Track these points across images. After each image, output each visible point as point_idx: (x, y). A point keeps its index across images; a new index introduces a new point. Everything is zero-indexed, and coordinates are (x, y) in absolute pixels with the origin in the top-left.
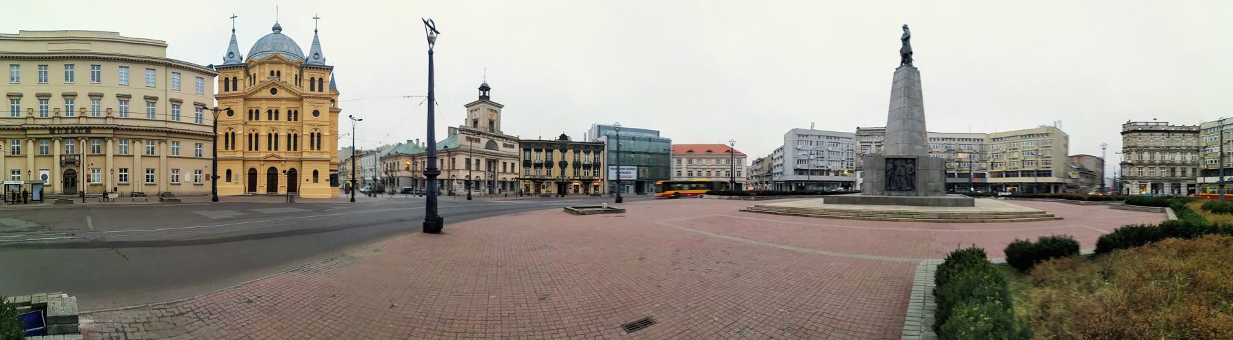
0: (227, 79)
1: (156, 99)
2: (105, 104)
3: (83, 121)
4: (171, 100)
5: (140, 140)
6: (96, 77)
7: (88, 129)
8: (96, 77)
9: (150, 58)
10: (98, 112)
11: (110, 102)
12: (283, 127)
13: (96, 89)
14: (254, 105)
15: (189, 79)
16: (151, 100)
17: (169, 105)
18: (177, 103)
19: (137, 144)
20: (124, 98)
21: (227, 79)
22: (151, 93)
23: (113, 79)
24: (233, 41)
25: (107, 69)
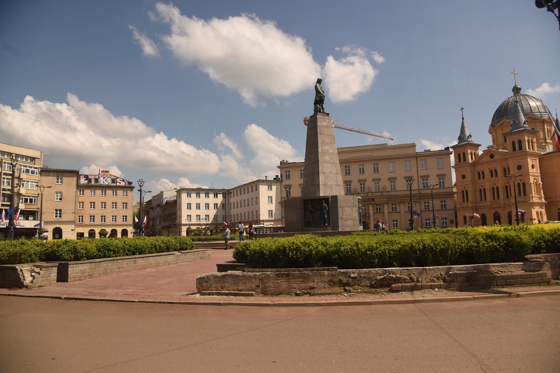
0: (459, 154)
1: (411, 177)
2: (382, 184)
3: (370, 195)
4: (421, 177)
5: (404, 203)
6: (376, 170)
7: (373, 200)
8: (376, 170)
9: (407, 154)
10: (379, 190)
11: (385, 184)
12: (500, 182)
13: (376, 176)
14: (480, 168)
15: (432, 162)
16: (409, 179)
17: (421, 180)
18: (425, 178)
19: (402, 205)
20: (392, 180)
21: (459, 154)
22: (408, 174)
23: (386, 170)
25: (382, 166)
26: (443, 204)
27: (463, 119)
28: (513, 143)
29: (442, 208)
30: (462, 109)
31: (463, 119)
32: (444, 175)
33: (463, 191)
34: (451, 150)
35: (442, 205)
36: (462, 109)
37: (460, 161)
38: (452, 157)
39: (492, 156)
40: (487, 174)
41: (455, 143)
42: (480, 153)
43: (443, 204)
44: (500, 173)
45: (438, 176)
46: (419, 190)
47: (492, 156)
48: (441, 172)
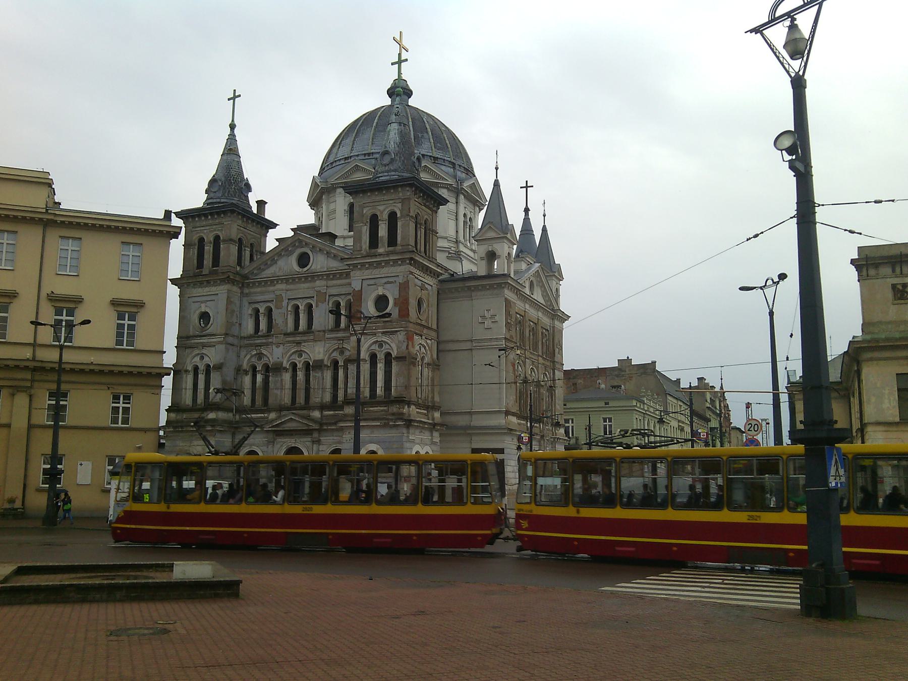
0: (201, 241)
4: (53, 298)
15: (102, 253)
18: (67, 304)
21: (201, 241)
24: (231, 150)
26: (121, 405)
27: (232, 127)
28: (374, 221)
29: (115, 420)
30: (235, 97)
31: (232, 127)
32: (140, 305)
33: (196, 369)
34: (176, 222)
35: (115, 410)
36: (235, 97)
37: (200, 264)
38: (177, 247)
39: (303, 260)
40: (284, 320)
41: (198, 200)
42: (271, 244)
43: (121, 405)
44: (322, 318)
45: (115, 303)
46: (34, 345)
47: (303, 260)
48: (128, 292)
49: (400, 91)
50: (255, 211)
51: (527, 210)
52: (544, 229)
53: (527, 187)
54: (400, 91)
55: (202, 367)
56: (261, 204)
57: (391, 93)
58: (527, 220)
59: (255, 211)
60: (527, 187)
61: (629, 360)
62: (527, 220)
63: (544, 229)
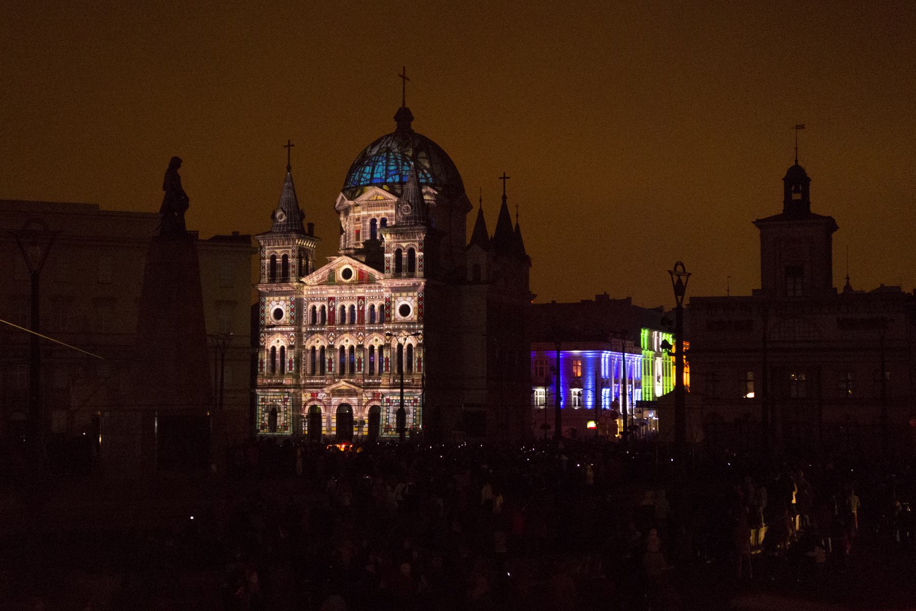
30: (289, 146)
31: (289, 168)
36: (289, 146)
49: (404, 116)
50: (307, 231)
51: (504, 198)
52: (517, 226)
53: (504, 178)
54: (404, 116)
55: (278, 349)
56: (311, 226)
57: (396, 118)
58: (504, 208)
59: (307, 231)
60: (504, 178)
61: (606, 296)
62: (504, 208)
63: (517, 226)
